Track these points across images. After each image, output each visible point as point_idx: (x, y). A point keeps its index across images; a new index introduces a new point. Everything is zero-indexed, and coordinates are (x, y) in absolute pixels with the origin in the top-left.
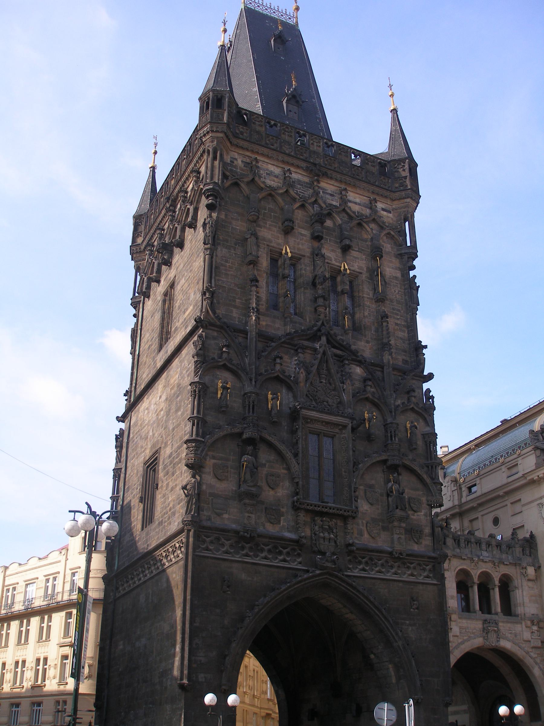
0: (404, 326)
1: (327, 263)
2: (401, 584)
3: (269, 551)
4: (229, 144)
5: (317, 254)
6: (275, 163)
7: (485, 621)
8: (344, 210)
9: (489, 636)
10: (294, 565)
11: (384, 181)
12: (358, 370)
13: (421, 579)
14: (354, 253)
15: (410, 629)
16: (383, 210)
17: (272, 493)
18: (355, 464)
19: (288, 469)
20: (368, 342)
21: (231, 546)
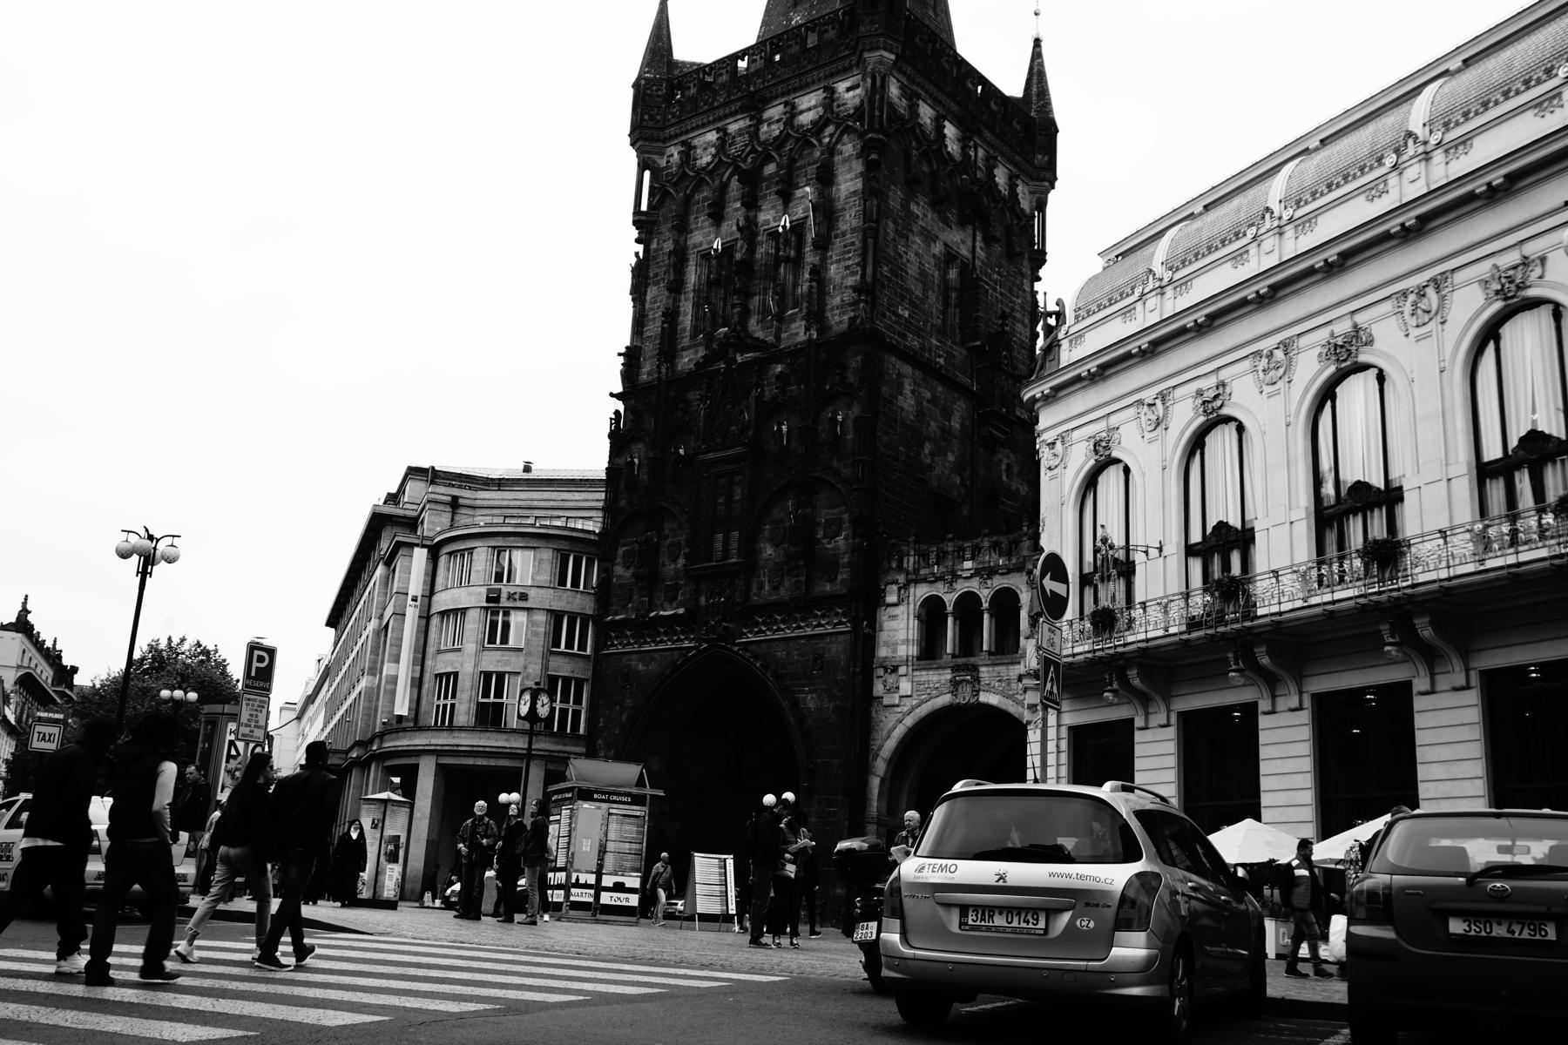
0: (857, 264)
1: (765, 230)
3: (665, 634)
4: (658, 144)
5: (749, 230)
6: (712, 127)
9: (960, 690)
10: (687, 644)
11: (848, 40)
12: (779, 368)
13: (829, 629)
14: (799, 193)
15: (810, 696)
16: (848, 90)
17: (672, 566)
21: (633, 636)
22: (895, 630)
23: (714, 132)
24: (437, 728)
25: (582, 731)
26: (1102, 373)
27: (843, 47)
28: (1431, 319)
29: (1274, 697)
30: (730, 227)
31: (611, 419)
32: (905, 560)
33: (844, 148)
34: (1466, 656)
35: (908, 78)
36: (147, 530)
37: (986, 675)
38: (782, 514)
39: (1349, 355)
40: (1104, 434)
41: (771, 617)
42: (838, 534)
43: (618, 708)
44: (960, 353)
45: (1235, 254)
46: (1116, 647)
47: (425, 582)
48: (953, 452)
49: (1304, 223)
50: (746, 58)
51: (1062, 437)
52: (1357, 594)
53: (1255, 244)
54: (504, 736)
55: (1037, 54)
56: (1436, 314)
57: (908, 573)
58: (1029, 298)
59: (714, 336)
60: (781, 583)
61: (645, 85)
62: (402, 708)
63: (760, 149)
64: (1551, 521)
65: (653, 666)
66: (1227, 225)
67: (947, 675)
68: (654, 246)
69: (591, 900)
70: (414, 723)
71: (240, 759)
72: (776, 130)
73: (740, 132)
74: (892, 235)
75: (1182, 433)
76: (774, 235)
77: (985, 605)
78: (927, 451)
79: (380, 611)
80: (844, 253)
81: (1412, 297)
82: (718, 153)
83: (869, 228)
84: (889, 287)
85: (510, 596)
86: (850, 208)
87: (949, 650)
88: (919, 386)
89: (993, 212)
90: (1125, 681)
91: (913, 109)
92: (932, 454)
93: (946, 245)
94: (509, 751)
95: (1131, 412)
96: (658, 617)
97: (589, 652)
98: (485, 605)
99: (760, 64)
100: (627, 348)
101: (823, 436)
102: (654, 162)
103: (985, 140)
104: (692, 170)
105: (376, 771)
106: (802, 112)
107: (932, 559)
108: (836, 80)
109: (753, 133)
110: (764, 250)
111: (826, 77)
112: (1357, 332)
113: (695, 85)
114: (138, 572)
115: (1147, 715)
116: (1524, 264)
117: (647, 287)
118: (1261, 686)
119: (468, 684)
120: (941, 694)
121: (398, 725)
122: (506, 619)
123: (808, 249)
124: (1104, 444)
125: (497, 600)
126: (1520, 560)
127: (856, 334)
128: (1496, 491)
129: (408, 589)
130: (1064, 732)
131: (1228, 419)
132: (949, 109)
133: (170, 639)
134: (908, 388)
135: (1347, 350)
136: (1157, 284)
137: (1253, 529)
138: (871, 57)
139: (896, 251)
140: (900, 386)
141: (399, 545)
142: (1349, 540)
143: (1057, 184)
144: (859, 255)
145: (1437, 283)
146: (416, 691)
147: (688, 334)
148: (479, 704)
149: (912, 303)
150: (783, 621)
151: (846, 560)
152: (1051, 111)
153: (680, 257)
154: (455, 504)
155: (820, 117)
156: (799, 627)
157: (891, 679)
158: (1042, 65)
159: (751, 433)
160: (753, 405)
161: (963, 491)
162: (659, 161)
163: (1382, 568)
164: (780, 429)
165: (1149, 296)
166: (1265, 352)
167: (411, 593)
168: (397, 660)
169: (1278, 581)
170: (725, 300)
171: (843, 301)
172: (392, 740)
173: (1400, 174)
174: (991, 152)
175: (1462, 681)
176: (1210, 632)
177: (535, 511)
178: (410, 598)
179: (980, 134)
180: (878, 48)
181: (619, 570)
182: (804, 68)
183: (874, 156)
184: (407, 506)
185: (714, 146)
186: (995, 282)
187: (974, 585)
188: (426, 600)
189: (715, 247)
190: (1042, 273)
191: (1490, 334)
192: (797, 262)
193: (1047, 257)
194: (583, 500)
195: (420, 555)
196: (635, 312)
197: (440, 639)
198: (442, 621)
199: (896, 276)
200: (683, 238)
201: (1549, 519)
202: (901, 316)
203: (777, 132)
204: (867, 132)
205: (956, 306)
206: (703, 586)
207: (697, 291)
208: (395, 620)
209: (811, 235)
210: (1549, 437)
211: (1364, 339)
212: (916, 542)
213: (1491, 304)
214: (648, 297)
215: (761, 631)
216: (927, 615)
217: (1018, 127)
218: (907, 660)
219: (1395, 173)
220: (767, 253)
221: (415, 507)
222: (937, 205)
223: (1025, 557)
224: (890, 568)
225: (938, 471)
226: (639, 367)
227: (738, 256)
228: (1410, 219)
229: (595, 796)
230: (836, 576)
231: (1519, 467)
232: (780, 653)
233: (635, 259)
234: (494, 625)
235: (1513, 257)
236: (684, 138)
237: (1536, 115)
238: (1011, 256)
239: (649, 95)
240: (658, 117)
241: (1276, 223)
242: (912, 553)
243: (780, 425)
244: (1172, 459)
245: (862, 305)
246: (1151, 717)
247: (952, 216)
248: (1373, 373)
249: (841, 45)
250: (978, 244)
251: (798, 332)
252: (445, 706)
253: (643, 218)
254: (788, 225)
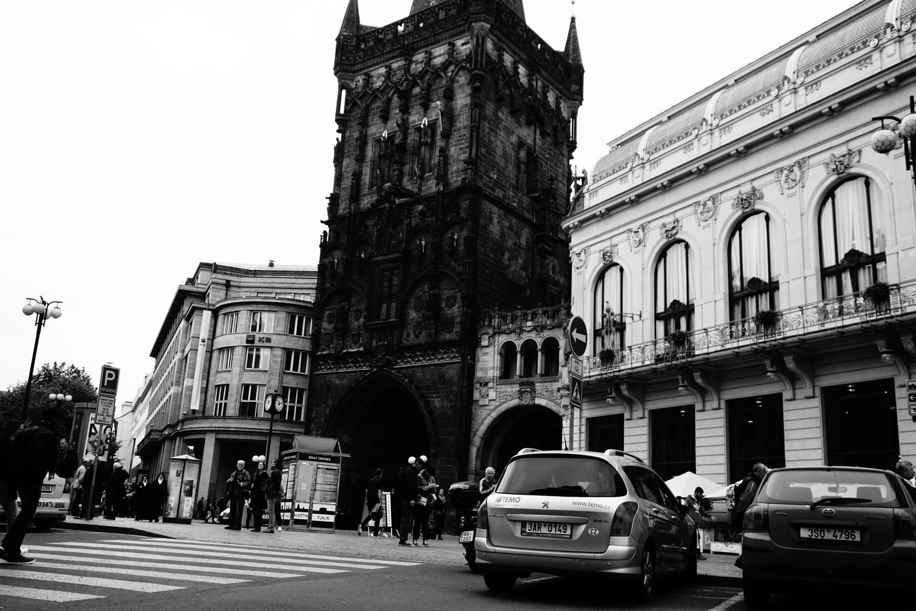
0: (467, 147)
1: (413, 126)
2: (433, 367)
3: (352, 362)
5: (404, 126)
6: (382, 65)
7: (521, 384)
8: (427, 71)
9: (524, 396)
11: (463, 15)
12: (420, 207)
13: (448, 361)
14: (433, 105)
16: (463, 45)
17: (357, 323)
21: (333, 364)
22: (487, 362)
23: (384, 68)
24: (216, 417)
25: (302, 419)
26: (609, 213)
27: (460, 19)
28: (796, 185)
29: (704, 402)
30: (392, 124)
31: (321, 236)
32: (493, 321)
33: (460, 79)
34: (813, 378)
35: (498, 39)
36: (42, 298)
37: (539, 388)
38: (421, 293)
39: (750, 205)
40: (609, 249)
41: (414, 353)
42: (454, 305)
43: (324, 406)
44: (526, 200)
45: (686, 145)
46: (614, 372)
47: (209, 331)
48: (521, 258)
49: (725, 128)
50: (403, 24)
51: (585, 250)
52: (752, 343)
53: (697, 140)
54: (256, 422)
55: (573, 27)
56: (799, 182)
57: (494, 328)
58: (567, 169)
59: (382, 188)
60: (420, 333)
61: (344, 38)
62: (195, 405)
63: (411, 78)
64: (862, 302)
65: (345, 382)
66: (681, 128)
67: (516, 388)
68: (348, 134)
69: (306, 518)
70: (203, 414)
71: (97, 435)
72: (420, 67)
73: (399, 68)
74: (487, 130)
75: (654, 249)
76: (418, 129)
77: (539, 347)
78: (506, 257)
79: (183, 348)
80: (459, 140)
81: (785, 172)
82: (386, 80)
83: (474, 126)
84: (485, 161)
85: (261, 340)
86: (463, 114)
87: (518, 373)
88: (502, 219)
89: (546, 118)
90: (619, 392)
91: (500, 57)
92: (509, 259)
93: (519, 137)
94: (259, 431)
95: (625, 236)
96: (347, 353)
97: (307, 373)
98: (246, 344)
99: (411, 28)
100: (331, 194)
101: (446, 247)
102: (348, 85)
103: (542, 76)
104: (370, 90)
105: (180, 442)
106: (435, 57)
107: (509, 320)
109: (407, 69)
110: (412, 138)
111: (450, 37)
112: (754, 191)
113: (372, 40)
114: (36, 323)
115: (631, 411)
116: (849, 154)
117: (343, 158)
118: (786, 383)
119: (235, 391)
120: (513, 399)
121: (193, 416)
122: (258, 353)
123: (438, 138)
124: (608, 254)
125: (253, 342)
126: (844, 324)
127: (465, 188)
128: (831, 283)
129: (199, 335)
130: (584, 421)
131: (680, 241)
132: (521, 57)
133: (55, 363)
134: (495, 220)
135: (749, 202)
136: (641, 162)
137: (693, 305)
138: (477, 26)
139: (490, 140)
140: (491, 219)
141: (194, 309)
142: (748, 309)
143: (583, 102)
144: (468, 142)
145: (800, 164)
146: (204, 395)
147: (367, 186)
148: (241, 403)
149: (499, 171)
150: (421, 356)
151: (458, 320)
152: (581, 60)
153: (363, 141)
154: (228, 285)
155: (446, 60)
156: (430, 359)
157: (484, 390)
158: (575, 33)
159: (404, 245)
160: (405, 229)
161: (527, 280)
162: (351, 84)
163: (766, 328)
164: (421, 243)
165: (635, 169)
166: (702, 202)
167: (202, 337)
168: (192, 377)
169: (707, 335)
170: (389, 167)
171: (458, 168)
172: (189, 424)
173: (780, 100)
174: (546, 83)
175: (810, 393)
176: (668, 364)
177: (276, 290)
178: (200, 340)
179: (539, 72)
180: (480, 21)
181: (325, 325)
182: (437, 31)
183: (477, 84)
184: (199, 286)
185: (383, 76)
186: (547, 159)
187: (533, 336)
188: (210, 341)
189: (384, 135)
190: (574, 154)
191: (830, 194)
192: (432, 145)
193: (577, 145)
194: (304, 284)
195: (207, 315)
196: (336, 173)
197: (218, 364)
198: (220, 354)
199: (489, 154)
200: (365, 130)
201: (861, 300)
202: (492, 178)
203: (421, 69)
204: (473, 70)
205: (524, 173)
206: (374, 335)
207: (373, 162)
208: (192, 353)
209: (440, 130)
210: (862, 253)
211: (758, 196)
212: (499, 310)
213: (830, 176)
214: (344, 164)
215: (408, 362)
216: (505, 352)
217: (561, 69)
218: (493, 379)
219: (777, 100)
220: (414, 140)
221: (204, 286)
222: (514, 113)
223: (562, 319)
224: (484, 325)
225: (512, 269)
226: (338, 205)
227: (397, 141)
228: (785, 127)
229: (310, 457)
230: (452, 331)
231: (844, 270)
232: (419, 374)
233: (336, 142)
234: (250, 357)
235: (843, 150)
236: (366, 71)
237: (857, 68)
238: (557, 144)
239: (345, 45)
240: (351, 58)
241: (709, 128)
242: (497, 316)
243: (421, 240)
244: (648, 263)
245: (469, 171)
246: (634, 413)
247: (523, 120)
248: (763, 215)
249: (459, 18)
250: (538, 137)
251: (432, 186)
252: (221, 404)
253: (341, 118)
254: (427, 123)
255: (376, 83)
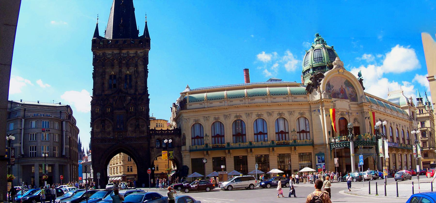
5: (120, 71)
10: (113, 143)
12: (130, 98)
14: (131, 68)
16: (140, 53)
17: (108, 130)
18: (127, 120)
19: (112, 124)
20: (133, 90)
63: (122, 58)
68: (97, 69)
73: (117, 54)
104: (106, 57)
106: (130, 54)
108: (138, 50)
162: (98, 54)
164: (132, 109)
203: (126, 56)
243: (131, 108)
255: (108, 56)
